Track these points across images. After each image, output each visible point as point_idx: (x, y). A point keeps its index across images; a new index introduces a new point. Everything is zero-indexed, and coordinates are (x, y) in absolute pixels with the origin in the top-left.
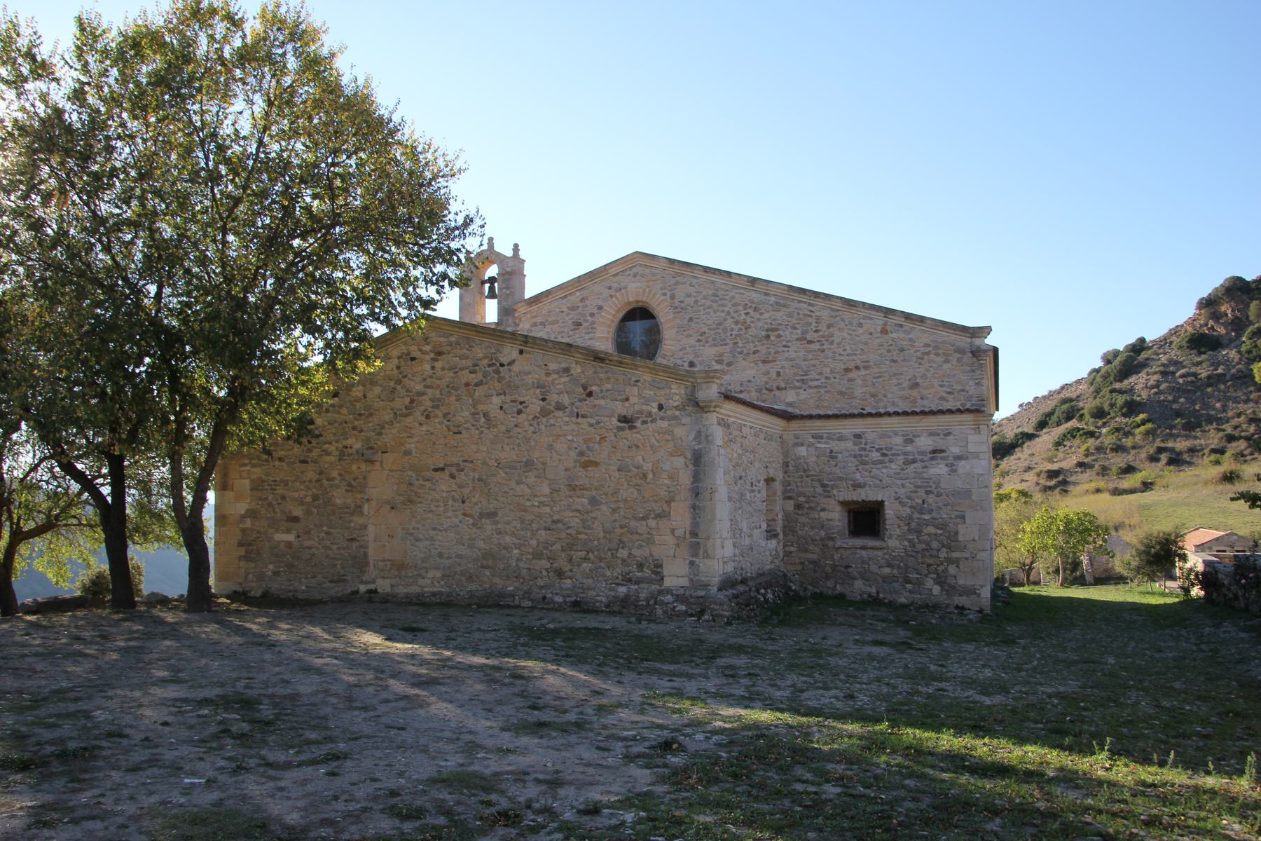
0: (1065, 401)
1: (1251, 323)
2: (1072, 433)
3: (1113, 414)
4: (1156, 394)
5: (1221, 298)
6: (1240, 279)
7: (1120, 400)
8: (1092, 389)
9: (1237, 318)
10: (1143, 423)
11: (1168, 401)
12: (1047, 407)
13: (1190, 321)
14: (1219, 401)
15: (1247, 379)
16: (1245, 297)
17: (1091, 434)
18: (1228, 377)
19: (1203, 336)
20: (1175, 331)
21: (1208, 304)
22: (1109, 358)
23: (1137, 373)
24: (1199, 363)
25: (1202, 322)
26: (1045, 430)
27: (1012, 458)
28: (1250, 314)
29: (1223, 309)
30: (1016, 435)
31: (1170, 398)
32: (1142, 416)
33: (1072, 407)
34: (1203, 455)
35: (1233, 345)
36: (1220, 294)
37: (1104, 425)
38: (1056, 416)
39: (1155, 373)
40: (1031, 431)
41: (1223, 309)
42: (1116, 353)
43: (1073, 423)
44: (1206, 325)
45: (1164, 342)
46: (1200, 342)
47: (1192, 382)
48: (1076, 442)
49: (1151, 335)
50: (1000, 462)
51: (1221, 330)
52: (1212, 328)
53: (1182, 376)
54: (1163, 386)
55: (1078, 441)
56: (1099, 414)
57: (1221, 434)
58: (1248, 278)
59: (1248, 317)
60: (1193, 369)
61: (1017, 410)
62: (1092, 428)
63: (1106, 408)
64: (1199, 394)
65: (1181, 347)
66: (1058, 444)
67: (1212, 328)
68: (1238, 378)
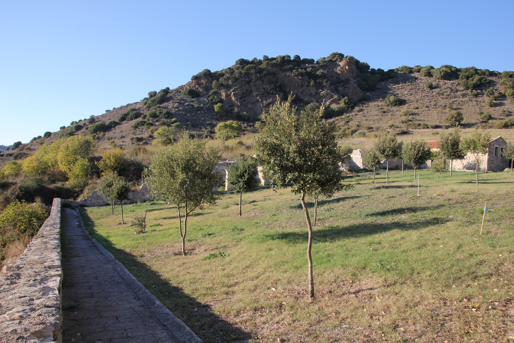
0: (133, 110)
1: (212, 89)
2: (143, 123)
3: (160, 116)
4: (177, 111)
5: (202, 77)
6: (209, 71)
7: (165, 111)
8: (145, 107)
9: (207, 86)
10: (175, 122)
11: (183, 115)
12: (126, 112)
13: (188, 84)
14: (202, 117)
15: (211, 111)
16: (210, 78)
17: (152, 125)
18: (205, 108)
19: (193, 90)
20: (182, 87)
21: (196, 78)
22: (153, 95)
23: (168, 102)
24: (193, 101)
25: (193, 85)
26: (124, 122)
27: (110, 132)
28: (213, 85)
29: (202, 81)
30: (111, 122)
31: (184, 113)
32: (174, 119)
33: (137, 112)
34: (203, 137)
35: (205, 96)
36: (202, 75)
37: (157, 121)
38: (130, 115)
39: (177, 102)
40: (117, 121)
41: (202, 81)
42: (155, 93)
43: (140, 119)
44: (195, 87)
45: (178, 91)
46: (193, 93)
47: (191, 108)
48: (145, 127)
49: (173, 87)
50: (105, 133)
51: (201, 90)
52: (197, 88)
53: (187, 105)
54: (181, 108)
55: (146, 127)
56: (154, 116)
57: (207, 130)
58: (212, 71)
59: (211, 86)
60: (191, 103)
61: (104, 112)
62: (151, 122)
63: (158, 113)
64: (194, 113)
65: (185, 94)
66: (136, 127)
67: (197, 88)
68: (208, 110)
